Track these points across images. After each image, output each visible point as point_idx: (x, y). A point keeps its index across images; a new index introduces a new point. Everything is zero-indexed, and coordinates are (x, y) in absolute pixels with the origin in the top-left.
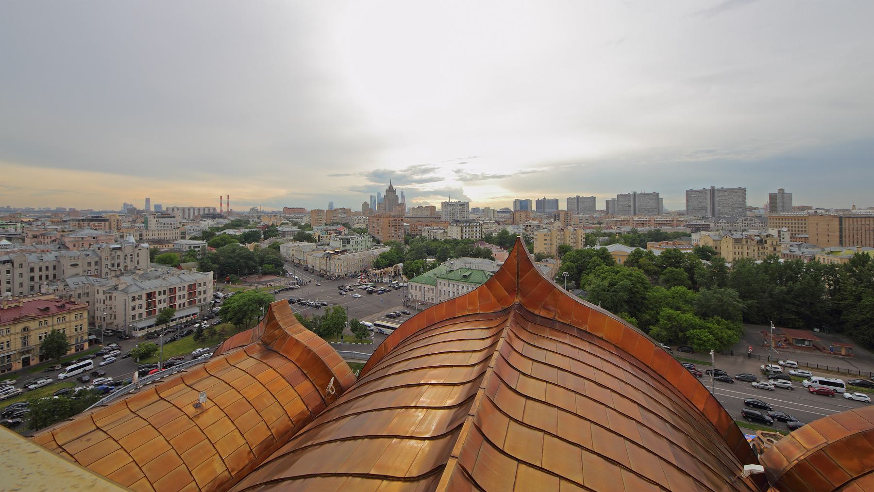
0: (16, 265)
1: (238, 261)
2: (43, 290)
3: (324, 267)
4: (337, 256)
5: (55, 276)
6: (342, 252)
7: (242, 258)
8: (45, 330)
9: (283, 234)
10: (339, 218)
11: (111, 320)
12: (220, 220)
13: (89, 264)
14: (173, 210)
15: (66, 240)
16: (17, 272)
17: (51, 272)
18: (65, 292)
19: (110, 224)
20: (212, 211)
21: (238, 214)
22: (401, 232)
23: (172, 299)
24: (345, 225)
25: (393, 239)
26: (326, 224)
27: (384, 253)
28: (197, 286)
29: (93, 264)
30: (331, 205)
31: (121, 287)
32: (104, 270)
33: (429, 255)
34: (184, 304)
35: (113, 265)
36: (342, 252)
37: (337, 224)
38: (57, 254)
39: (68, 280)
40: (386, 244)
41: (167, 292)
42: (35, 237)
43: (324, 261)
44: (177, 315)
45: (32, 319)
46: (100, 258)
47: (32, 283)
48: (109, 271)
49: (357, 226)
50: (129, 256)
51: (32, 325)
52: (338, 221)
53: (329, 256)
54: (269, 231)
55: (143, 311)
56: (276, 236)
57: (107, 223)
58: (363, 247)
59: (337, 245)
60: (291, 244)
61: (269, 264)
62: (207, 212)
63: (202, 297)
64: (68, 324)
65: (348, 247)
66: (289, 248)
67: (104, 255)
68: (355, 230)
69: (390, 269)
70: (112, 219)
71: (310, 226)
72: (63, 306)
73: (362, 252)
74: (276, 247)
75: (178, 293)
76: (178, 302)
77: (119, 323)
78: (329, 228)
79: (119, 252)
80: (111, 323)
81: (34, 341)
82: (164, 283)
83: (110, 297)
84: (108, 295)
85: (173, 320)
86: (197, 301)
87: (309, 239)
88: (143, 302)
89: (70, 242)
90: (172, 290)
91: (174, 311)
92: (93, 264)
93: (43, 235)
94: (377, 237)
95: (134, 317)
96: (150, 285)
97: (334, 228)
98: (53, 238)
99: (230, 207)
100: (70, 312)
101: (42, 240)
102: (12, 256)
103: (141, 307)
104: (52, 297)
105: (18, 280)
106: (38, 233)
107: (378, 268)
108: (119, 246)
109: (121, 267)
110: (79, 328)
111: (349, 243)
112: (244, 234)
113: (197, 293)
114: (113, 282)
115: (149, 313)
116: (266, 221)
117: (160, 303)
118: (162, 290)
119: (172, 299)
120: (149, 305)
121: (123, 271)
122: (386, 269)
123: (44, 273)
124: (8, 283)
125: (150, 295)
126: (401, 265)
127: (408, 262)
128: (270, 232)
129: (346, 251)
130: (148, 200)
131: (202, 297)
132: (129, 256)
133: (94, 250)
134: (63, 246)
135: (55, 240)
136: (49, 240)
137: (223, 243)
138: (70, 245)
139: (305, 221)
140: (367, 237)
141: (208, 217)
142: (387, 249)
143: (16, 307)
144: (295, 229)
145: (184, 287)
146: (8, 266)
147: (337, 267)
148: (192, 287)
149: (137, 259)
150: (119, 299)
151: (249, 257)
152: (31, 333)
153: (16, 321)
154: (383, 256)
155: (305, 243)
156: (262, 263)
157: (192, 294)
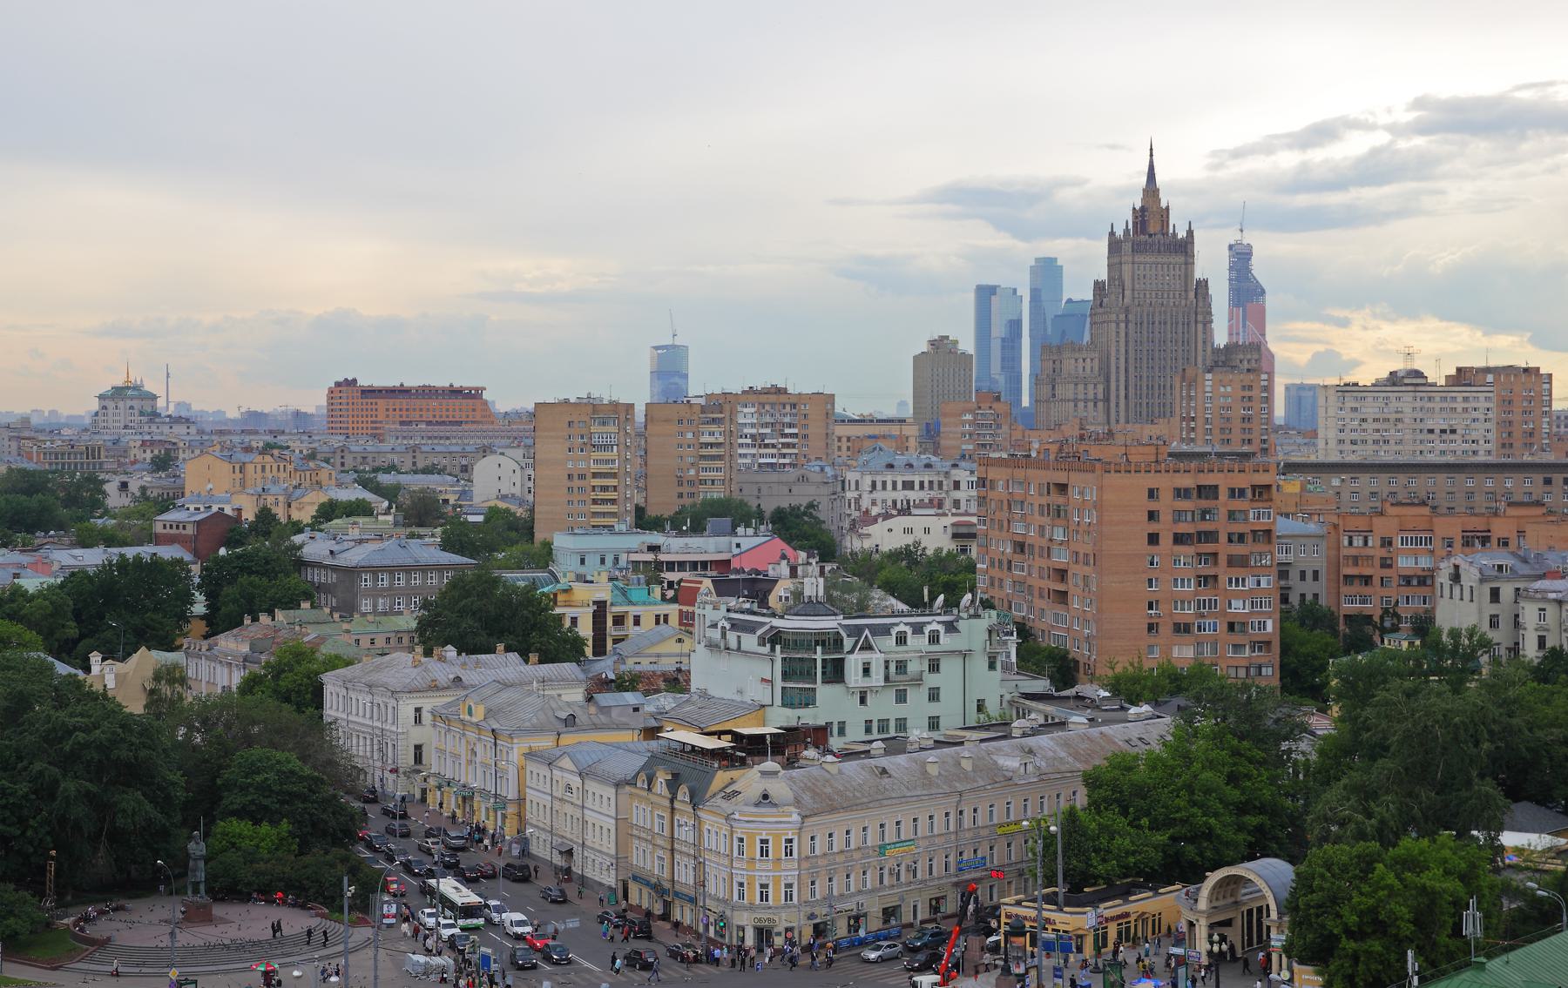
1: (46, 791)
3: (648, 861)
4: (752, 779)
6: (785, 746)
10: (748, 467)
22: (1251, 600)
24: (799, 529)
25: (1183, 654)
26: (643, 521)
27: (1124, 764)
30: (669, 365)
33: (1515, 794)
36: (785, 746)
37: (736, 514)
40: (1128, 690)
43: (647, 813)
49: (886, 537)
52: (739, 490)
53: (689, 774)
54: (244, 565)
56: (291, 603)
58: (951, 712)
59: (737, 681)
60: (404, 666)
61: (254, 815)
65: (830, 704)
66: (395, 712)
68: (870, 569)
69: (1167, 902)
71: (526, 529)
73: (945, 753)
74: (295, 688)
78: (676, 546)
87: (530, 630)
94: (1054, 627)
97: (708, 546)
107: (1079, 889)
111: (835, 672)
122: (1144, 903)
126: (1269, 877)
127: (1342, 852)
128: (252, 570)
129: (819, 736)
139: (494, 481)
140: (974, 631)
142: (1145, 730)
144: (427, 549)
147: (758, 857)
151: (121, 755)
154: (1115, 789)
155: (504, 665)
156: (205, 804)
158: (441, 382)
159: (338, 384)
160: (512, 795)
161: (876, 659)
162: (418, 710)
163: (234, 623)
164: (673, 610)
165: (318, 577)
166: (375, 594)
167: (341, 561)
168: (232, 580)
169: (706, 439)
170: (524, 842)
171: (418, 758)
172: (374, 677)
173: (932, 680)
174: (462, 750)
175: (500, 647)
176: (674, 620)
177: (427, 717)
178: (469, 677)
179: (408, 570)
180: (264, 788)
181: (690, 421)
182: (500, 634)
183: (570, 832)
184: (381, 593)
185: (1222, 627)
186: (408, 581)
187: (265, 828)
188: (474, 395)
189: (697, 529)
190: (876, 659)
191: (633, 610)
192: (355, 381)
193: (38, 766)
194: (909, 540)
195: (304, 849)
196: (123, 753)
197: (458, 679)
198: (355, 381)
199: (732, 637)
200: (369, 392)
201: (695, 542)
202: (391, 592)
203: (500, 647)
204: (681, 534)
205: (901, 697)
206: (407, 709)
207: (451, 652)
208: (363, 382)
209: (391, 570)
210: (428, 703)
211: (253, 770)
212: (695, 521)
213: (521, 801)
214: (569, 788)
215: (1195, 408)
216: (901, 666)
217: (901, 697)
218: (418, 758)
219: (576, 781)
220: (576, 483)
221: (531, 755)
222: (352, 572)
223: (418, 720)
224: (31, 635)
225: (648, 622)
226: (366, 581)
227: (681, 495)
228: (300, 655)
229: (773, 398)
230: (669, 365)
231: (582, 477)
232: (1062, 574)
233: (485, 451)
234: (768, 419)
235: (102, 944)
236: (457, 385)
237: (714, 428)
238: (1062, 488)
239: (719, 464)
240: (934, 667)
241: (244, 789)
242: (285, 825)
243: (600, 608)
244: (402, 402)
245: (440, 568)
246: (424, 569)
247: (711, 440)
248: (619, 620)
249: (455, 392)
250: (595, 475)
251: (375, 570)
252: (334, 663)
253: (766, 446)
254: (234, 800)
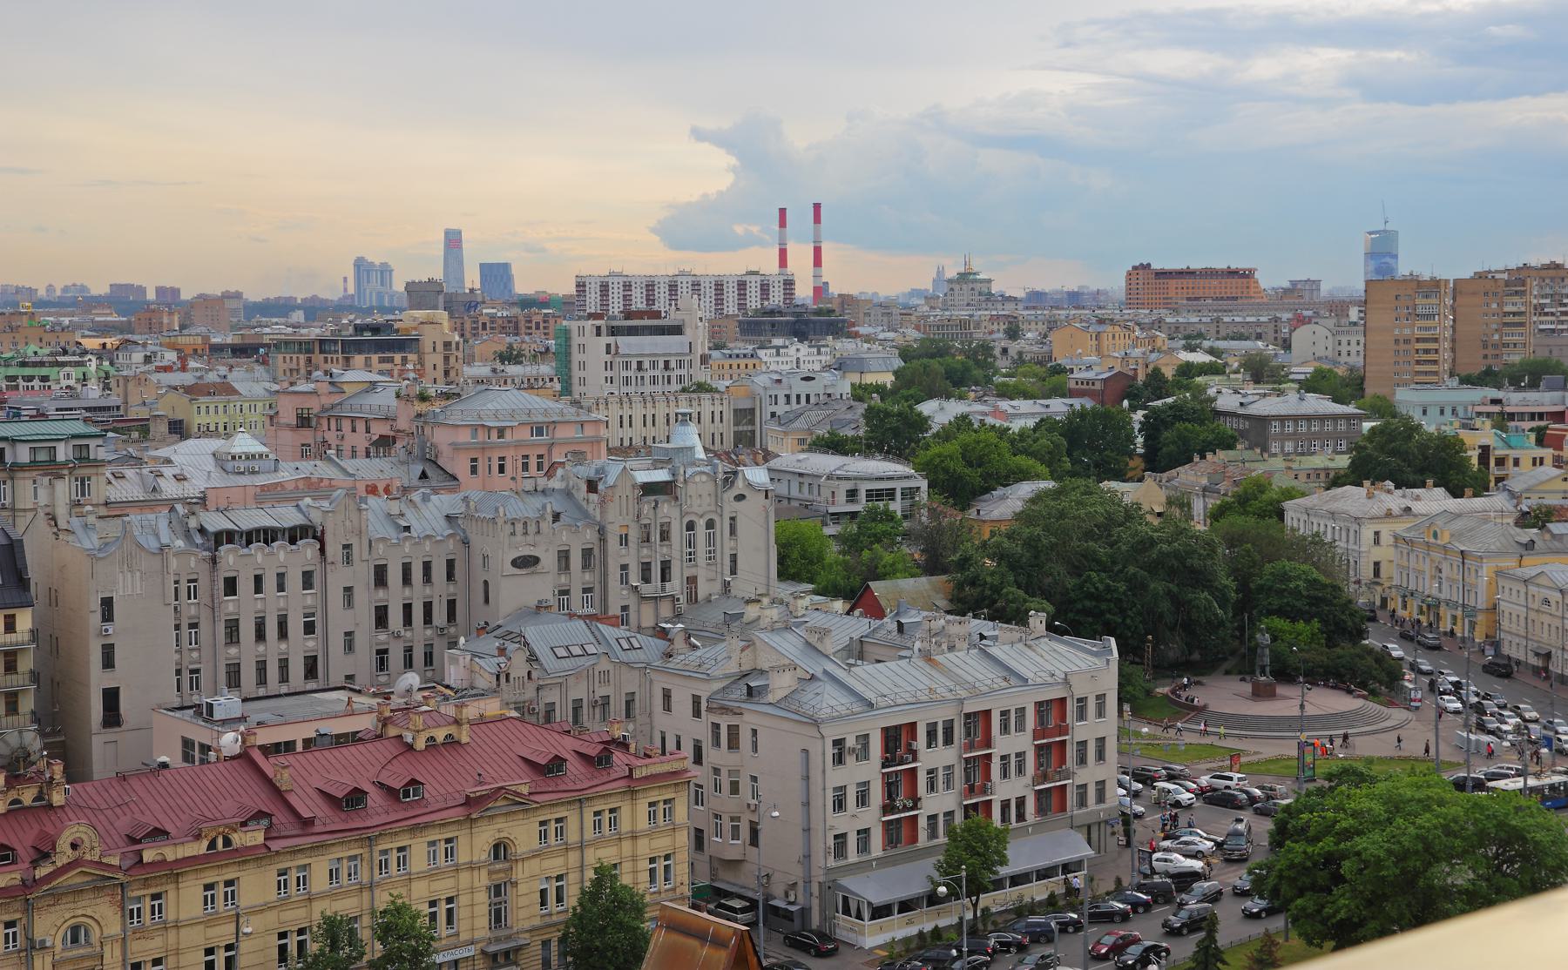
0: (334, 550)
1: (1137, 586)
2: (454, 675)
5: (452, 604)
7: (1153, 568)
8: (555, 865)
9: (1258, 430)
11: (733, 848)
12: (846, 346)
13: (564, 556)
14: (604, 288)
15: (441, 438)
16: (338, 578)
17: (440, 590)
18: (530, 693)
19: (421, 362)
20: (777, 298)
21: (887, 311)
23: (977, 771)
26: (1467, 381)
28: (1071, 707)
29: (576, 560)
30: (1381, 249)
31: (781, 684)
32: (618, 597)
34: (1021, 802)
35: (646, 569)
38: (444, 502)
39: (531, 632)
41: (959, 731)
42: (304, 421)
44: (1021, 855)
45: (520, 805)
46: (602, 532)
47: (383, 637)
48: (632, 601)
50: (701, 524)
51: (523, 833)
54: (1177, 413)
55: (871, 817)
57: (412, 357)
60: (1352, 498)
61: (1292, 615)
62: (754, 301)
63: (1088, 775)
64: (626, 846)
66: (1372, 533)
67: (618, 518)
70: (429, 337)
72: (598, 762)
75: (1003, 744)
76: (1004, 789)
77: (779, 864)
78: (1516, 400)
79: (667, 510)
80: (734, 864)
81: (525, 912)
82: (941, 684)
83: (733, 731)
84: (724, 722)
85: (998, 885)
86: (1071, 798)
87: (1442, 466)
88: (871, 770)
89: (456, 447)
90: (978, 723)
91: (1001, 837)
92: (576, 560)
93: (332, 415)
95: (841, 839)
96: (901, 685)
98: (379, 429)
99: (827, 273)
100: (633, 786)
101: (331, 437)
102: (314, 510)
103: (863, 799)
104: (492, 707)
105: (339, 620)
106: (314, 405)
108: (661, 476)
109: (676, 586)
110: (660, 865)
112: (1045, 424)
113: (1071, 752)
114: (724, 658)
115: (893, 834)
116: (1091, 363)
117: (932, 787)
118: (940, 716)
119: (977, 771)
120: (890, 788)
121: (683, 599)
123: (418, 594)
124: (309, 628)
125: (897, 740)
130: (453, 241)
131: (1088, 775)
132: (701, 524)
133: (568, 494)
134: (434, 472)
135: (385, 443)
136: (360, 440)
137: (973, 475)
138: (461, 467)
141: (776, 329)
143: (452, 743)
145: (1021, 712)
146: (307, 550)
148: (1052, 713)
149: (729, 545)
150: (773, 755)
152: (521, 872)
153: (474, 806)
155: (1432, 500)
157: (1051, 754)
158: (1221, 265)
160: (1482, 604)
162: (1377, 533)
163: (1183, 457)
164: (1547, 453)
165: (1228, 426)
166: (1283, 437)
167: (1254, 410)
168: (1167, 425)
169: (1508, 308)
170: (1496, 645)
171: (1377, 573)
172: (1334, 506)
174: (1427, 567)
175: (1430, 482)
176: (1548, 461)
177: (1386, 538)
178: (1417, 507)
179: (1309, 418)
180: (1296, 593)
181: (1495, 294)
182: (1422, 471)
184: (1289, 437)
186: (1309, 428)
187: (1301, 625)
188: (1246, 275)
189: (1534, 385)
191: (1513, 454)
193: (1132, 569)
195: (1331, 643)
196: (1195, 562)
197: (1408, 509)
200: (1162, 274)
201: (1532, 396)
202: (1312, 437)
203: (1430, 482)
204: (1519, 389)
206: (1367, 534)
207: (1390, 484)
208: (1157, 265)
209: (1296, 419)
210: (1386, 531)
211: (1284, 577)
212: (1533, 375)
213: (1494, 608)
214: (1547, 602)
218: (1377, 573)
220: (1402, 346)
221: (1499, 573)
222: (1263, 421)
223: (1377, 542)
224: (1042, 469)
225: (1526, 463)
226: (1275, 428)
228: (1261, 487)
230: (1381, 249)
231: (1407, 341)
233: (1301, 321)
235: (1202, 709)
236: (1233, 267)
237: (1516, 299)
239: (1521, 330)
241: (1280, 593)
242: (1316, 624)
243: (1485, 451)
244: (1188, 282)
245: (1335, 418)
246: (1322, 418)
247: (1514, 309)
248: (1501, 462)
249: (1232, 273)
251: (1282, 419)
252: (1289, 494)
254: (1276, 602)
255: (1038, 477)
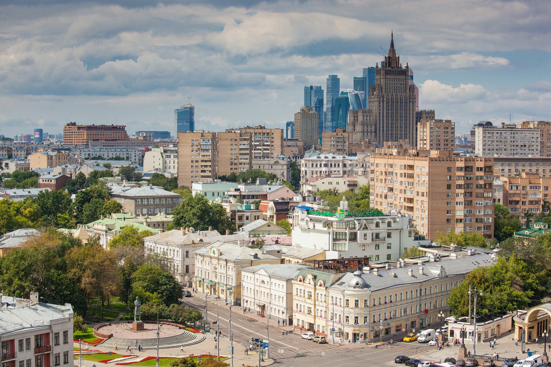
26: (223, 179)
158: (109, 124)
159: (68, 125)
161: (369, 233)
162: (187, 252)
173: (388, 240)
175: (210, 228)
179: (154, 198)
183: (264, 300)
184: (145, 206)
185: (474, 220)
186: (154, 202)
188: (122, 129)
190: (369, 233)
192: (75, 123)
194: (331, 187)
197: (201, 240)
198: (75, 123)
199: (311, 225)
203: (210, 228)
204: (247, 184)
205: (377, 247)
209: (148, 198)
215: (426, 135)
216: (377, 236)
217: (377, 247)
219: (266, 279)
220: (195, 164)
227: (231, 169)
229: (260, 131)
231: (197, 161)
232: (411, 200)
234: (258, 139)
236: (115, 125)
238: (411, 167)
240: (389, 236)
244: (94, 132)
245: (166, 197)
246: (160, 198)
249: (114, 128)
250: (202, 161)
253: (258, 149)
255: (28, 227)
